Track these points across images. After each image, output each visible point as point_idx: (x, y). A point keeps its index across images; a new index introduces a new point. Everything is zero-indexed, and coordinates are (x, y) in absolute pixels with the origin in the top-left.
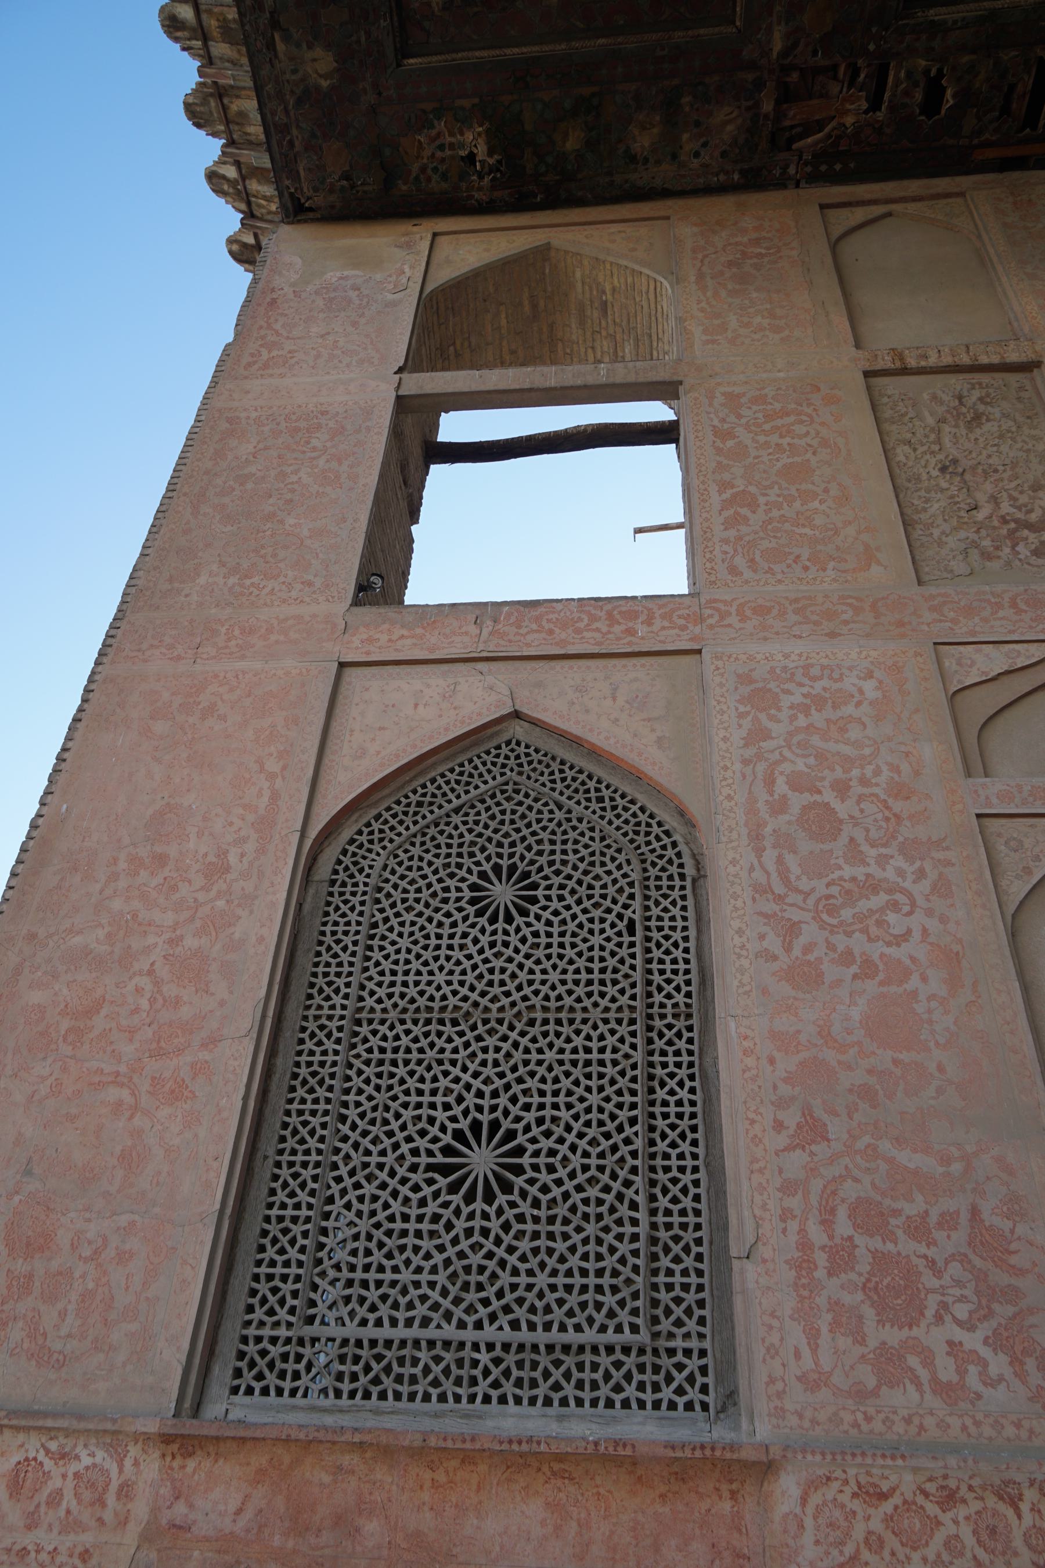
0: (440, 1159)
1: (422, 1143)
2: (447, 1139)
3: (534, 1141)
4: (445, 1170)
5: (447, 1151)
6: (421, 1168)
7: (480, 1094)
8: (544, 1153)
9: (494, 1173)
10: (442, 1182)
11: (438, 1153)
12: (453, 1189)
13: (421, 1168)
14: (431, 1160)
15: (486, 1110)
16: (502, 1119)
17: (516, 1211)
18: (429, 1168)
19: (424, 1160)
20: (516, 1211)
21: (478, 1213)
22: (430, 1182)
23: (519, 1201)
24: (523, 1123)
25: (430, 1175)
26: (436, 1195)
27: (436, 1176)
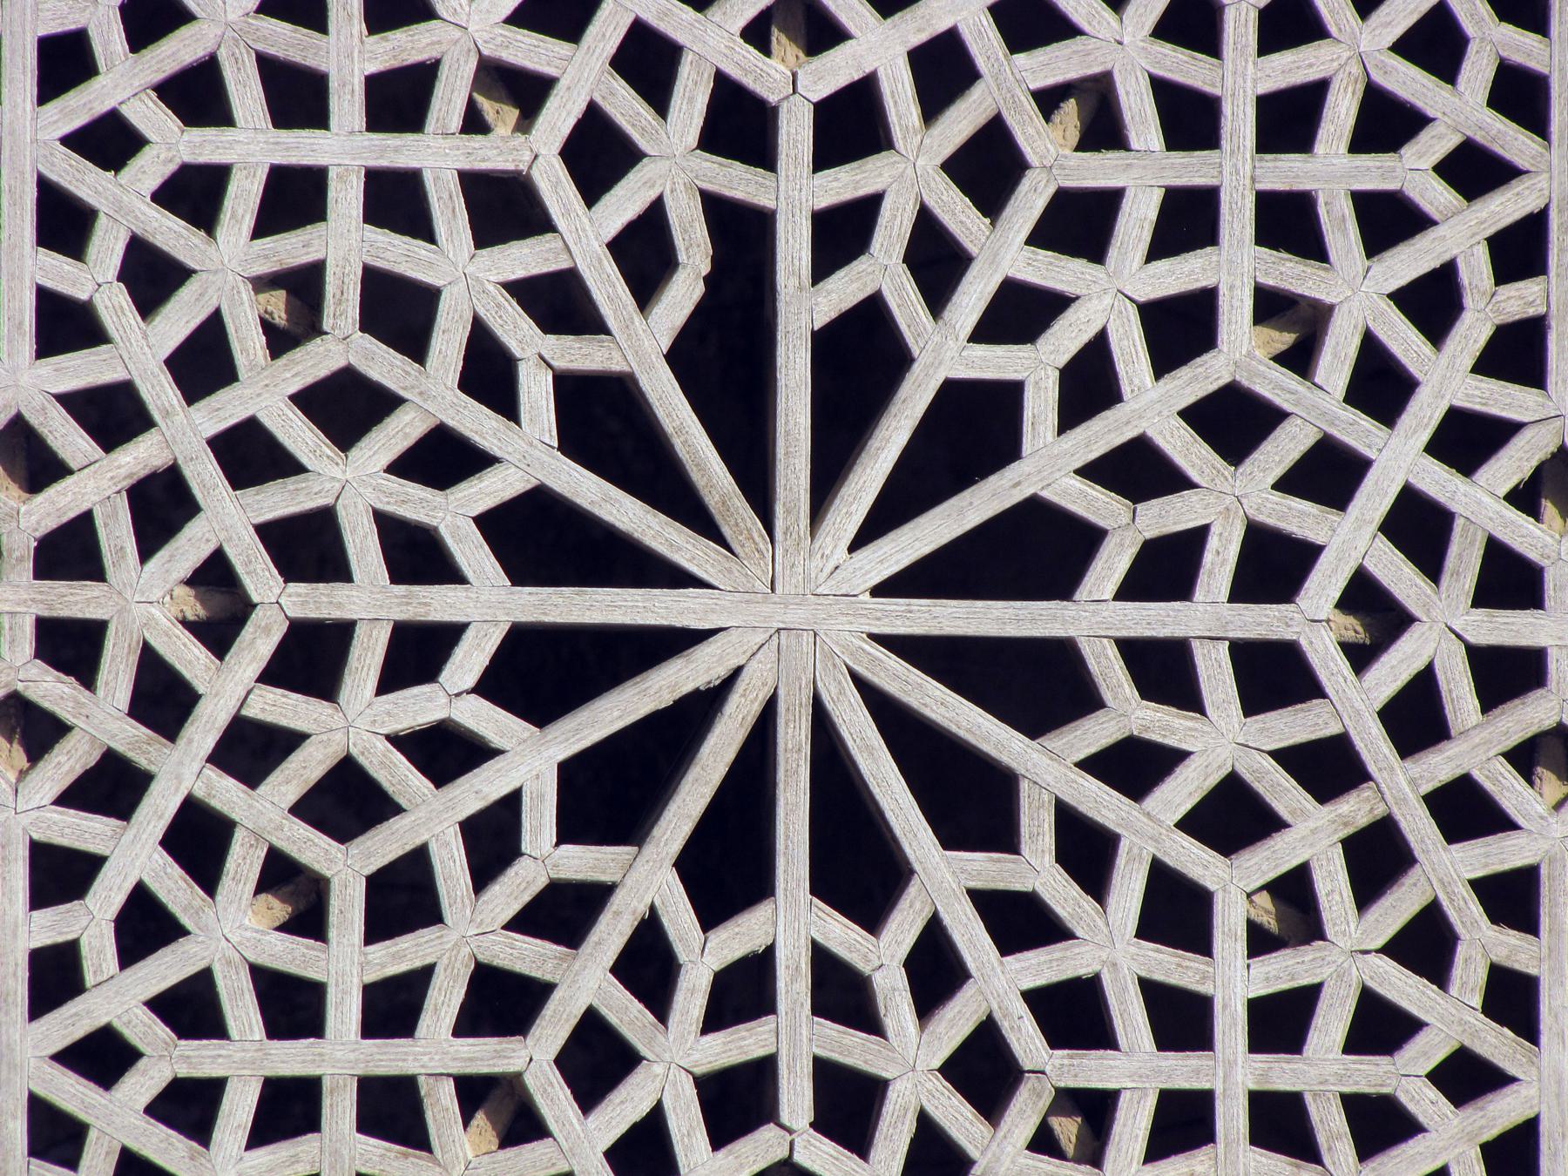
0: (804, 305)
1: (911, 172)
2: (944, 350)
3: (935, 973)
4: (725, 355)
5: (861, 356)
6: (738, 181)
7: (1273, 566)
8: (849, 1047)
9: (702, 707)
10: (639, 343)
11: (845, 290)
12: (601, 419)
13: (738, 181)
14: (793, 247)
15: (1155, 619)
16: (1092, 735)
17: (451, 867)
18: (741, 233)
19: (795, 192)
20: (451, 867)
21: (433, 603)
22: (644, 252)
23: (518, 886)
24: (1061, 893)
25: (694, 251)
26: (558, 303)
27: (683, 294)
